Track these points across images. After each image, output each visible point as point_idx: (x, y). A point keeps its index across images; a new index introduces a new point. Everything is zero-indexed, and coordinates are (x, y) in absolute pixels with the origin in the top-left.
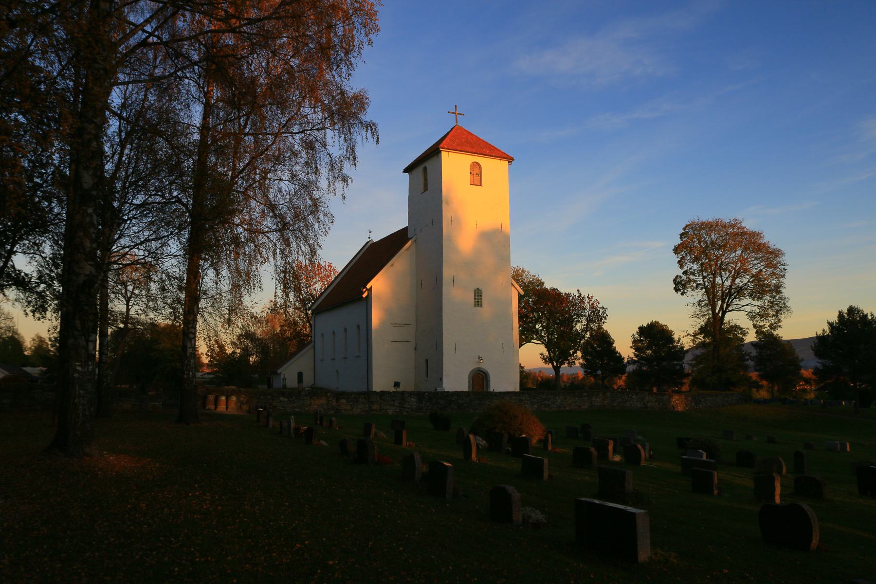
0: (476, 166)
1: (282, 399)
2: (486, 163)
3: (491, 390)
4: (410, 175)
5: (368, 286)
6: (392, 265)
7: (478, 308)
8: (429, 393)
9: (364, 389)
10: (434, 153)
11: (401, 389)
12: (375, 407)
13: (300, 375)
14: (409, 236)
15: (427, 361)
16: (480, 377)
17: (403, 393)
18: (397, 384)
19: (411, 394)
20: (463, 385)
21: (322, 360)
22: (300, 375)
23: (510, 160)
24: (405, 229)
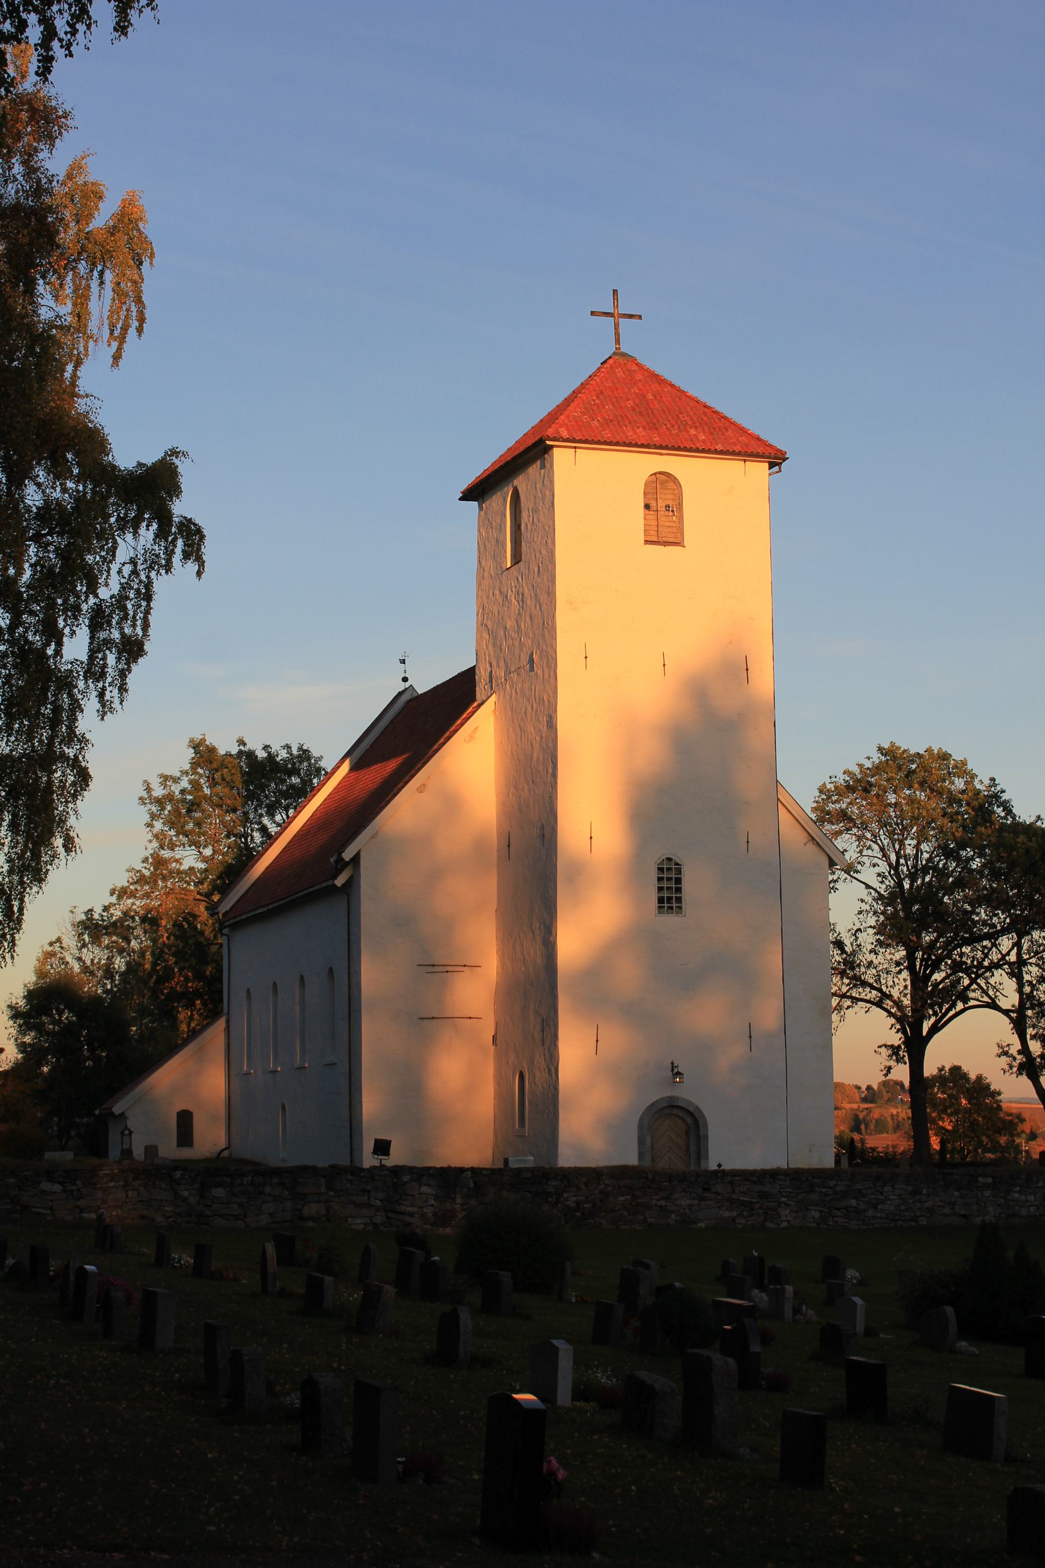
1: (46, 1186)
2: (699, 476)
3: (713, 1166)
4: (481, 508)
5: (348, 855)
6: (421, 789)
7: (671, 920)
10: (533, 452)
12: (312, 1209)
17: (397, 1171)
23: (776, 459)
24: (471, 671)
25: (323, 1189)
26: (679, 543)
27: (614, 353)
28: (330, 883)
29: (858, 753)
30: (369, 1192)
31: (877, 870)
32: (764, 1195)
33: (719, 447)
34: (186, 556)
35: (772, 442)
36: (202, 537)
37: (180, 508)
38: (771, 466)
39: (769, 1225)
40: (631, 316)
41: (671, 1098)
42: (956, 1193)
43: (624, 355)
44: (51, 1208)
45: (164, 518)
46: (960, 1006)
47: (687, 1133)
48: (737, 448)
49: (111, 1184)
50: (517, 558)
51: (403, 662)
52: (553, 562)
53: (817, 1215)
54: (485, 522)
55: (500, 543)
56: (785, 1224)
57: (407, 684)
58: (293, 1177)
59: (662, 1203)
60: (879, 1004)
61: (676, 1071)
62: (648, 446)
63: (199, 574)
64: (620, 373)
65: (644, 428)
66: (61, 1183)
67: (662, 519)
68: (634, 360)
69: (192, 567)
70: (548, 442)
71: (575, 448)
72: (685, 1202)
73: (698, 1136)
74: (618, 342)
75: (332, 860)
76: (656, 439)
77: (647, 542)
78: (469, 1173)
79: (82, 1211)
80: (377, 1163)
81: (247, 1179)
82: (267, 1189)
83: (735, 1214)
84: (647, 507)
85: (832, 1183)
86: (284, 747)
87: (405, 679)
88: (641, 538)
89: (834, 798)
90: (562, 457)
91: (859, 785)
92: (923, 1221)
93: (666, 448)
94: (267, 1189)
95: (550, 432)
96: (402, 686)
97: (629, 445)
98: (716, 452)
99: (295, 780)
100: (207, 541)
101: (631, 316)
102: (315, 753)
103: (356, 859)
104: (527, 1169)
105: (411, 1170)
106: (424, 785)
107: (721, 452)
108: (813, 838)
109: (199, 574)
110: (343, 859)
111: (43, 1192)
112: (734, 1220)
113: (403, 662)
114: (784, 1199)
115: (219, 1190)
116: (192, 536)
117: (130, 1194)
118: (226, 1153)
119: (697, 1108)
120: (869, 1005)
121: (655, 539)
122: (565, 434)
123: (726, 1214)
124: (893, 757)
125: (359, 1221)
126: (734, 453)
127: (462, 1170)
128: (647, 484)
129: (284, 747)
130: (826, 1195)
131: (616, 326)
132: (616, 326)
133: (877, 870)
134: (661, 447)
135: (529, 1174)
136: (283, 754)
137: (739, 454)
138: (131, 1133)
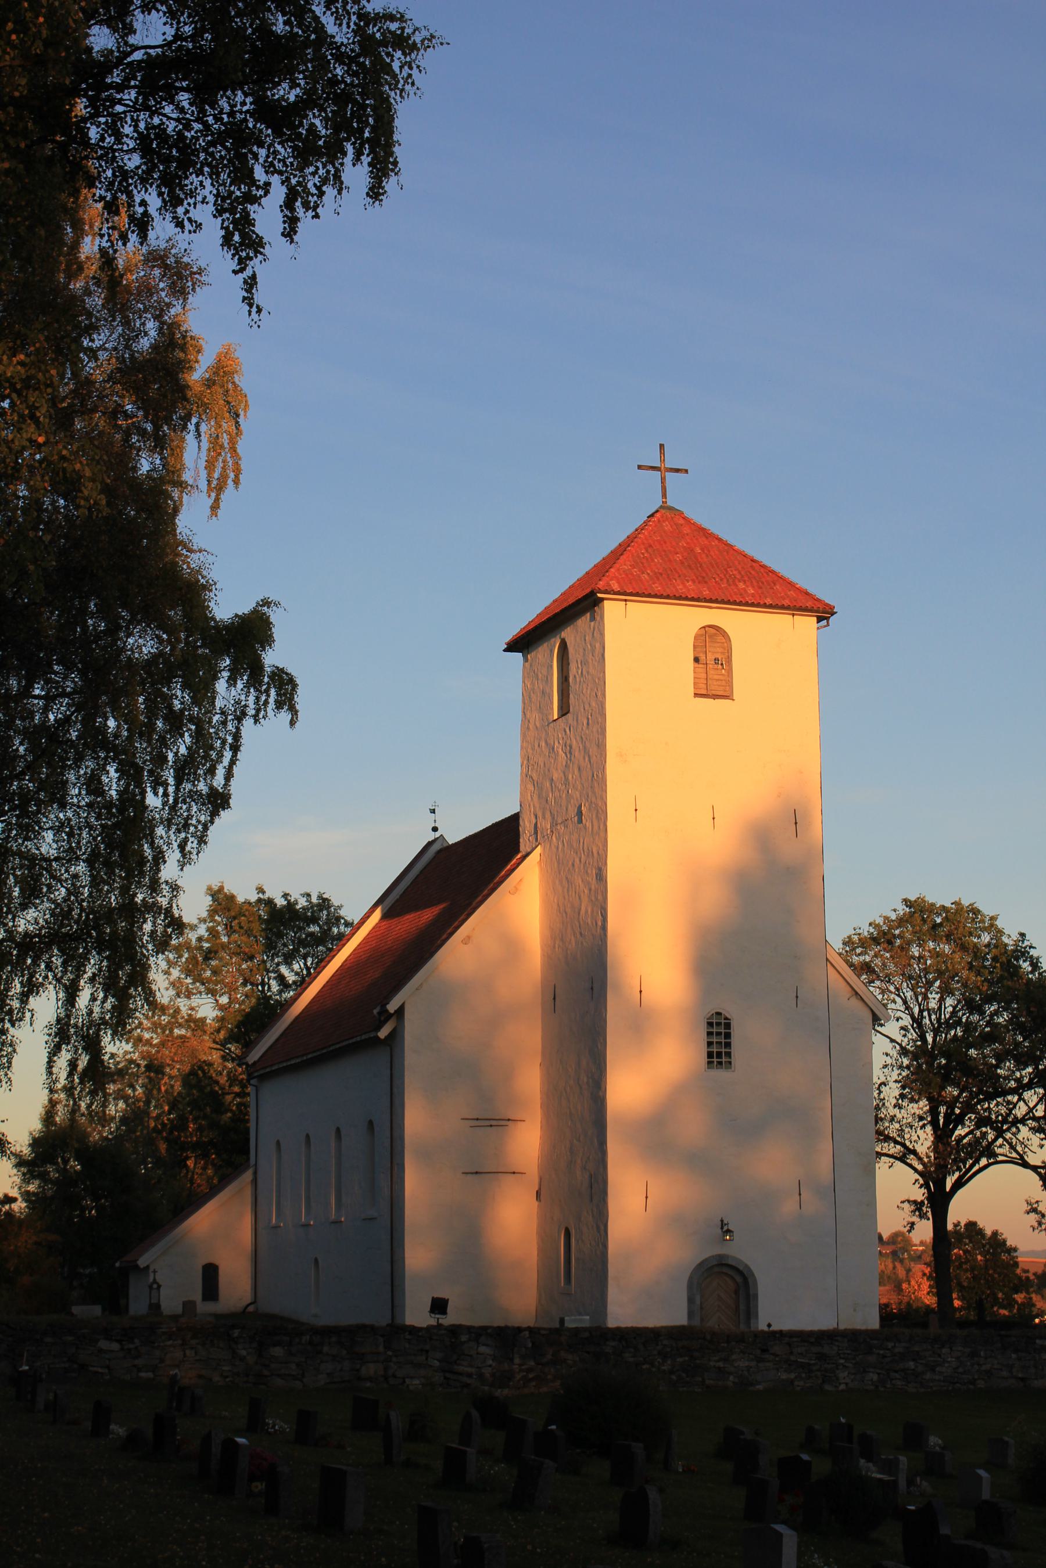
1: (103, 1344)
2: (749, 629)
3: (762, 1326)
4: (526, 660)
5: (392, 1007)
6: (467, 940)
9: (382, 1320)
10: (581, 605)
11: (447, 1320)
12: (370, 1369)
17: (455, 1330)
19: (479, 1333)
23: (824, 613)
25: (381, 1349)
26: (728, 696)
27: (661, 507)
28: (372, 1035)
29: (887, 906)
30: (427, 1351)
31: (901, 1023)
33: (768, 601)
34: (279, 705)
35: (819, 596)
36: (295, 686)
37: (271, 658)
38: (820, 619)
39: (828, 1387)
40: (677, 471)
42: (1014, 1356)
43: (671, 509)
44: (108, 1367)
45: (256, 669)
46: (984, 1161)
47: (736, 1292)
48: (786, 602)
49: (170, 1343)
50: (564, 710)
51: (433, 811)
52: (603, 715)
53: (875, 1377)
54: (529, 674)
55: (547, 695)
56: (842, 1387)
57: (438, 834)
58: (348, 1337)
59: (721, 1364)
60: (902, 1159)
61: (725, 1228)
62: (698, 600)
63: (292, 723)
64: (667, 526)
65: (693, 581)
66: (119, 1341)
67: (711, 672)
68: (681, 513)
69: (285, 716)
70: (599, 595)
71: (626, 600)
72: (743, 1364)
73: (748, 1296)
74: (664, 495)
75: (375, 1012)
76: (706, 593)
77: (696, 695)
78: (527, 1333)
79: (139, 1370)
80: (433, 1322)
81: (306, 1338)
82: (326, 1349)
83: (792, 1376)
84: (696, 660)
85: (890, 1345)
86: (303, 895)
87: (435, 829)
88: (692, 691)
89: (858, 951)
90: (612, 610)
91: (882, 937)
92: (981, 1384)
93: (716, 601)
94: (326, 1349)
95: (601, 584)
96: (432, 835)
97: (680, 598)
98: (765, 606)
99: (314, 928)
100: (300, 690)
101: (677, 471)
102: (335, 902)
103: (400, 1011)
104: (585, 1329)
105: (469, 1329)
106: (469, 937)
107: (771, 606)
108: (857, 993)
109: (292, 723)
110: (387, 1011)
111: (101, 1350)
112: (792, 1382)
113: (433, 811)
114: (842, 1361)
116: (284, 686)
117: (188, 1352)
118: (251, 1309)
119: (746, 1266)
120: (892, 1160)
121: (704, 692)
122: (616, 587)
123: (784, 1376)
124: (918, 911)
126: (783, 607)
127: (519, 1330)
128: (696, 637)
129: (303, 895)
130: (884, 1357)
131: (663, 480)
132: (663, 480)
133: (901, 1023)
134: (711, 601)
135: (587, 1335)
136: (302, 902)
137: (788, 608)
138: (159, 1286)
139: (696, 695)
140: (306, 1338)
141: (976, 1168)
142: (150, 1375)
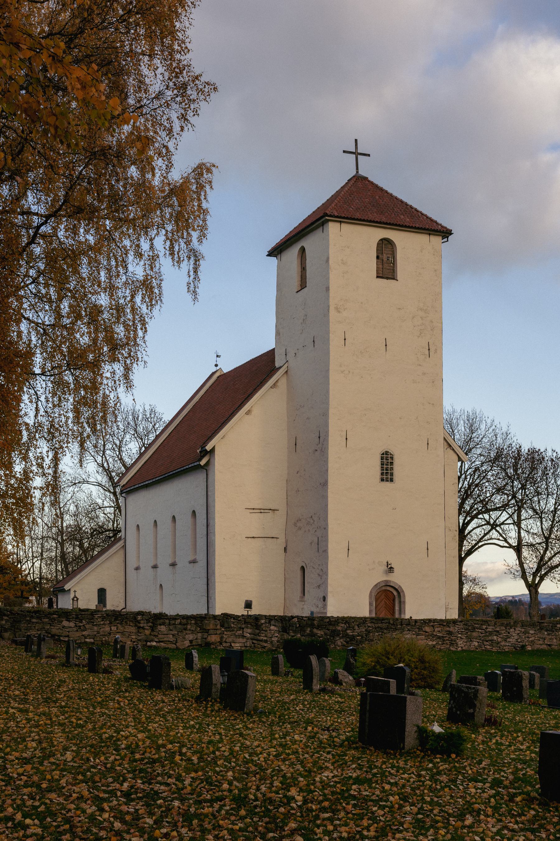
0: (386, 248)
1: (65, 623)
5: (208, 447)
6: (248, 413)
8: (300, 618)
11: (254, 611)
13: (102, 593)
14: (277, 365)
15: (303, 569)
16: (388, 596)
17: (257, 618)
18: (248, 605)
19: (270, 619)
20: (363, 609)
21: (137, 569)
22: (102, 593)
25: (218, 627)
30: (243, 629)
32: (450, 633)
41: (386, 581)
49: (102, 623)
53: (476, 644)
57: (218, 368)
61: (389, 566)
75: (198, 451)
79: (86, 638)
80: (245, 613)
81: (178, 621)
85: (484, 627)
87: (216, 365)
94: (189, 627)
96: (215, 369)
103: (213, 450)
108: (450, 446)
111: (64, 627)
112: (434, 646)
115: (162, 626)
117: (113, 628)
119: (400, 587)
123: (430, 643)
125: (238, 645)
127: (293, 617)
138: (78, 599)
139: (377, 277)
140: (178, 621)
141: (480, 544)
142: (92, 640)
